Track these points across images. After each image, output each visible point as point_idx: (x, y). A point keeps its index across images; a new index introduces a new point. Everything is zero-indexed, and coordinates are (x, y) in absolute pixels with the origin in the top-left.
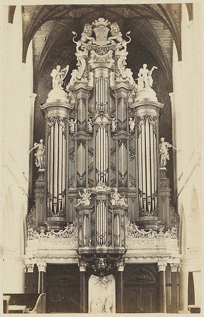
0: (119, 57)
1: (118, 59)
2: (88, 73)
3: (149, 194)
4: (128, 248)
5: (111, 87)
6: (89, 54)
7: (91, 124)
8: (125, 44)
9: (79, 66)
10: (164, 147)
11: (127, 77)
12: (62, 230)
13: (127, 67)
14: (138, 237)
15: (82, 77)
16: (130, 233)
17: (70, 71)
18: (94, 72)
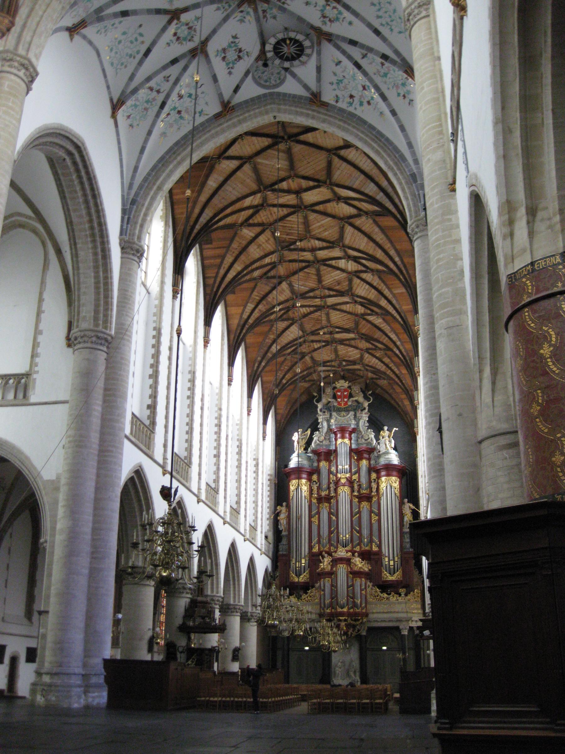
1: (359, 420)
3: (391, 558)
6: (331, 415)
8: (366, 404)
13: (369, 428)
17: (312, 434)
18: (336, 435)
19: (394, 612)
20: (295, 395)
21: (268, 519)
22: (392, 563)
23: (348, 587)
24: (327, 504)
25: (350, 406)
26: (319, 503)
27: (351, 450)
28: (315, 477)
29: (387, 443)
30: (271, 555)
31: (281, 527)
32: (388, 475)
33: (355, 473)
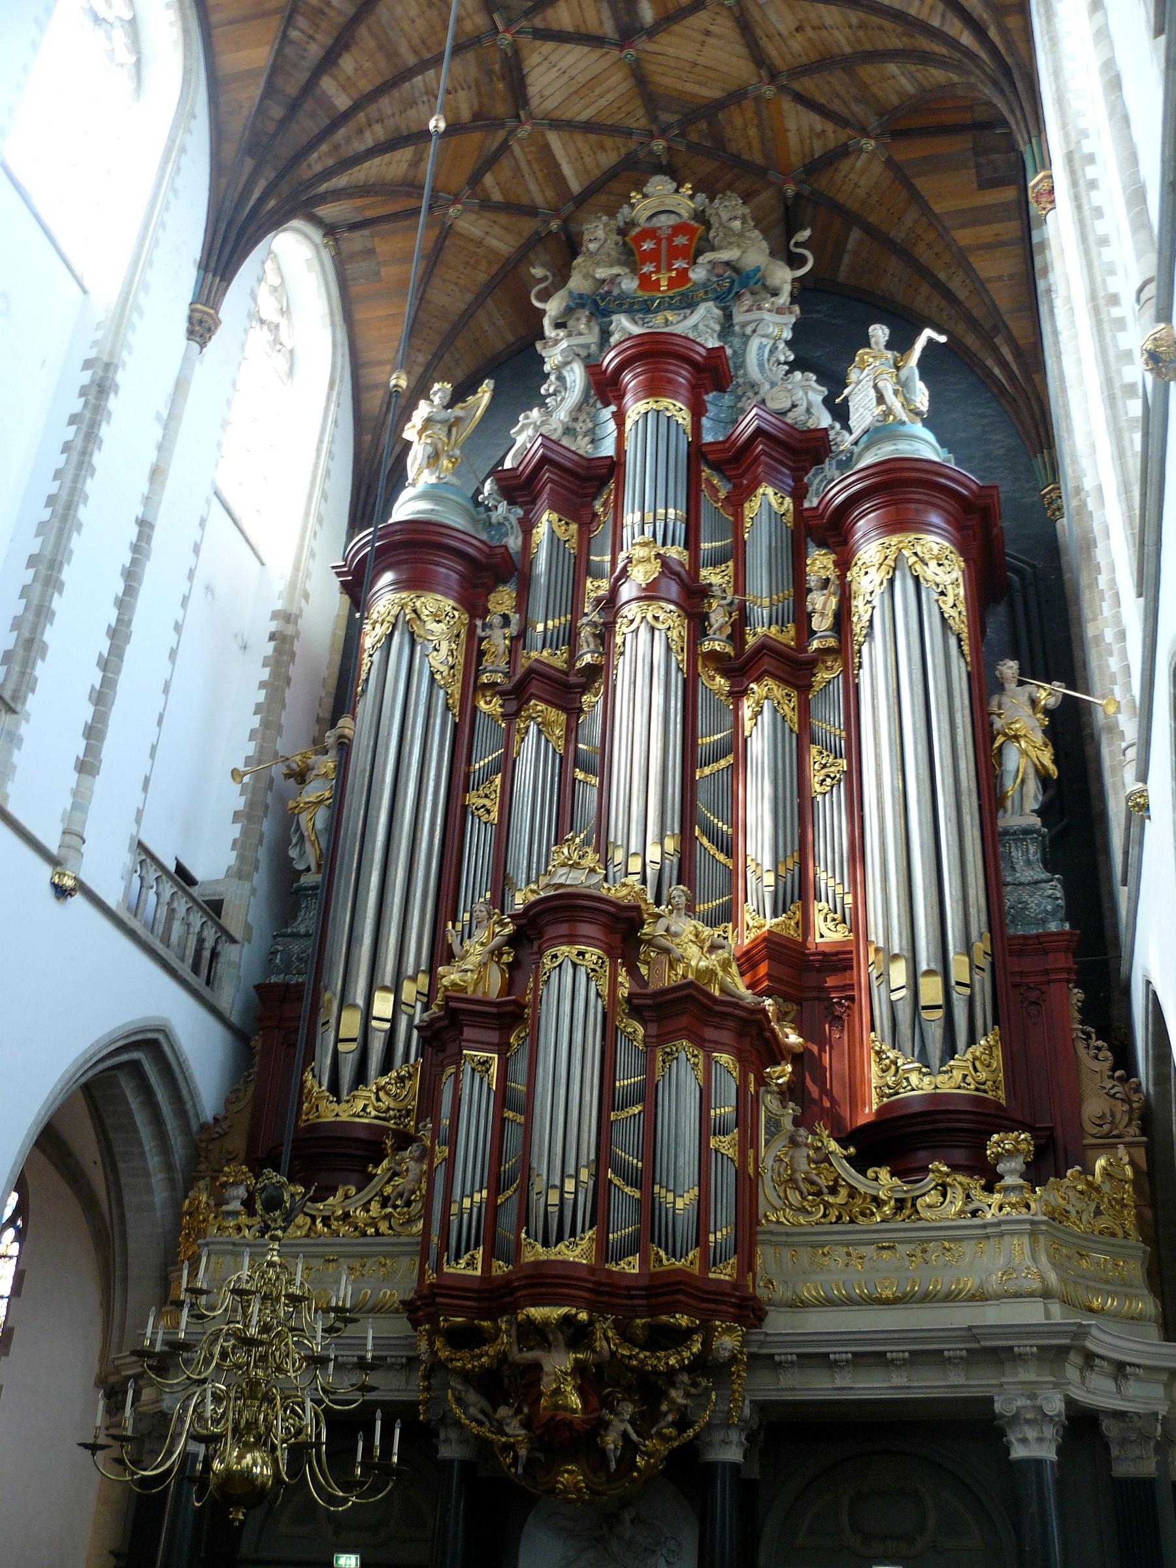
0: (754, 331)
1: (746, 339)
2: (594, 418)
4: (781, 1292)
5: (704, 449)
6: (605, 334)
7: (595, 625)
8: (783, 277)
9: (554, 394)
10: (1024, 708)
11: (794, 406)
12: (353, 1190)
13: (794, 366)
14: (852, 1221)
15: (564, 434)
16: (794, 1197)
19: (950, 1297)
20: (450, 297)
21: (237, 816)
22: (931, 990)
23: (608, 1099)
24: (556, 716)
25: (705, 285)
26: (510, 717)
27: (698, 454)
28: (503, 600)
29: (888, 388)
30: (229, 996)
31: (307, 857)
32: (895, 525)
33: (717, 560)
